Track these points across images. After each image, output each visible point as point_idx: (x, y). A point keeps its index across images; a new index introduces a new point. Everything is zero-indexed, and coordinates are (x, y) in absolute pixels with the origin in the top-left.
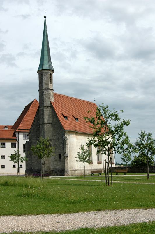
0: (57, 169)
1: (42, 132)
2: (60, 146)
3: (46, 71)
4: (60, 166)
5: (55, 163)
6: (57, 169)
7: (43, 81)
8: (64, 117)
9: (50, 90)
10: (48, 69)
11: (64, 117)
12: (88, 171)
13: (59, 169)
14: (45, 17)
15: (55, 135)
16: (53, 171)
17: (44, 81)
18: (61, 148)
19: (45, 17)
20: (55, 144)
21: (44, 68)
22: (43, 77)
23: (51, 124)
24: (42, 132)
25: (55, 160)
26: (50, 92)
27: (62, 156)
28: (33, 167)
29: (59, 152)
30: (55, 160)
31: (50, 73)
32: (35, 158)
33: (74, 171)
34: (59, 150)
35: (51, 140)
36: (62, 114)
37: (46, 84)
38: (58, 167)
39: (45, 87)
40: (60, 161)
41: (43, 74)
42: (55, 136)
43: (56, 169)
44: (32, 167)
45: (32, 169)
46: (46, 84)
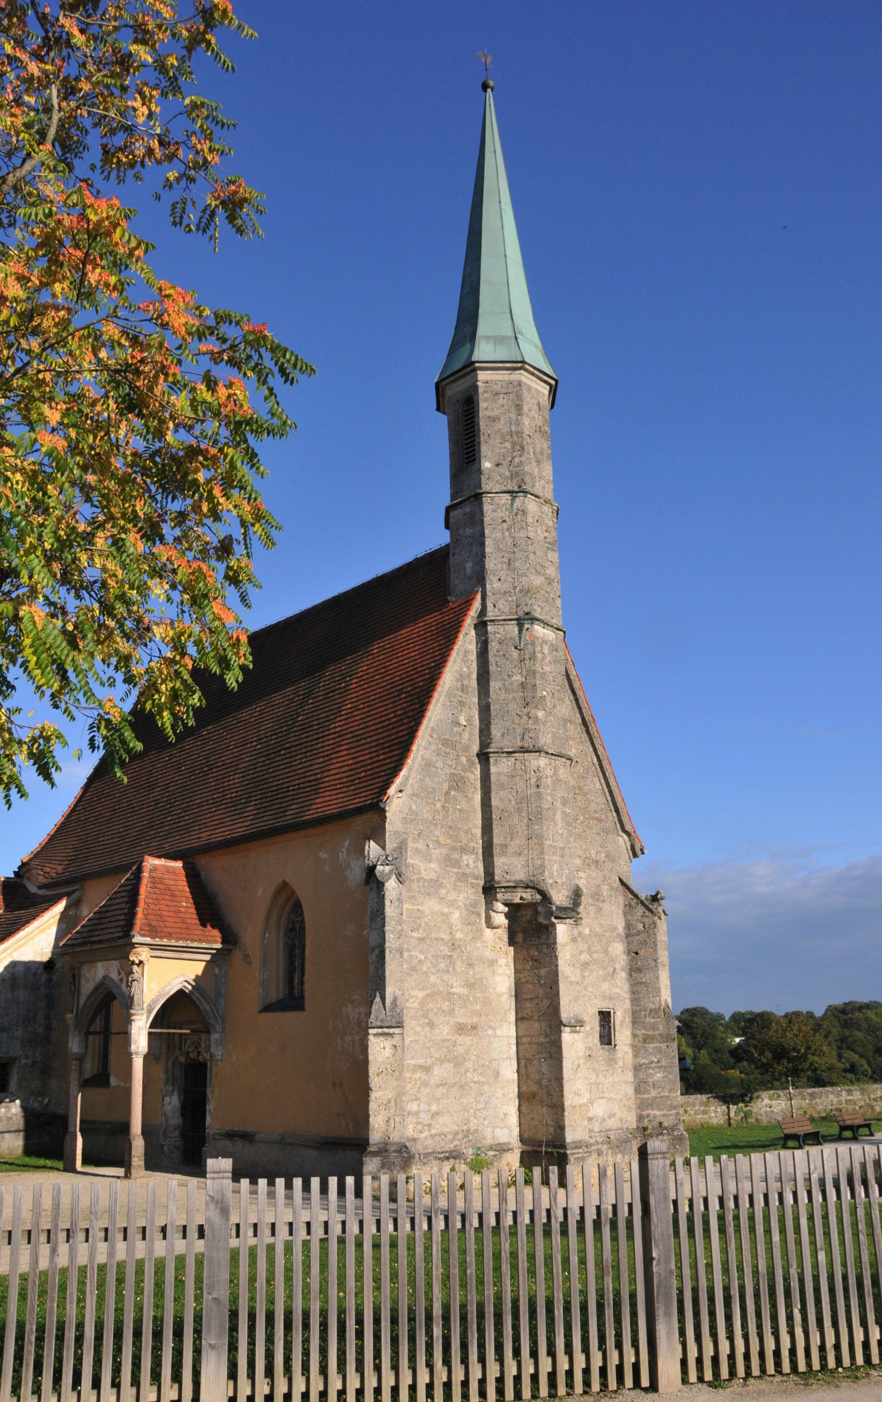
2: (606, 952)
18: (618, 966)
29: (604, 997)
32: (431, 1024)
40: (611, 1061)
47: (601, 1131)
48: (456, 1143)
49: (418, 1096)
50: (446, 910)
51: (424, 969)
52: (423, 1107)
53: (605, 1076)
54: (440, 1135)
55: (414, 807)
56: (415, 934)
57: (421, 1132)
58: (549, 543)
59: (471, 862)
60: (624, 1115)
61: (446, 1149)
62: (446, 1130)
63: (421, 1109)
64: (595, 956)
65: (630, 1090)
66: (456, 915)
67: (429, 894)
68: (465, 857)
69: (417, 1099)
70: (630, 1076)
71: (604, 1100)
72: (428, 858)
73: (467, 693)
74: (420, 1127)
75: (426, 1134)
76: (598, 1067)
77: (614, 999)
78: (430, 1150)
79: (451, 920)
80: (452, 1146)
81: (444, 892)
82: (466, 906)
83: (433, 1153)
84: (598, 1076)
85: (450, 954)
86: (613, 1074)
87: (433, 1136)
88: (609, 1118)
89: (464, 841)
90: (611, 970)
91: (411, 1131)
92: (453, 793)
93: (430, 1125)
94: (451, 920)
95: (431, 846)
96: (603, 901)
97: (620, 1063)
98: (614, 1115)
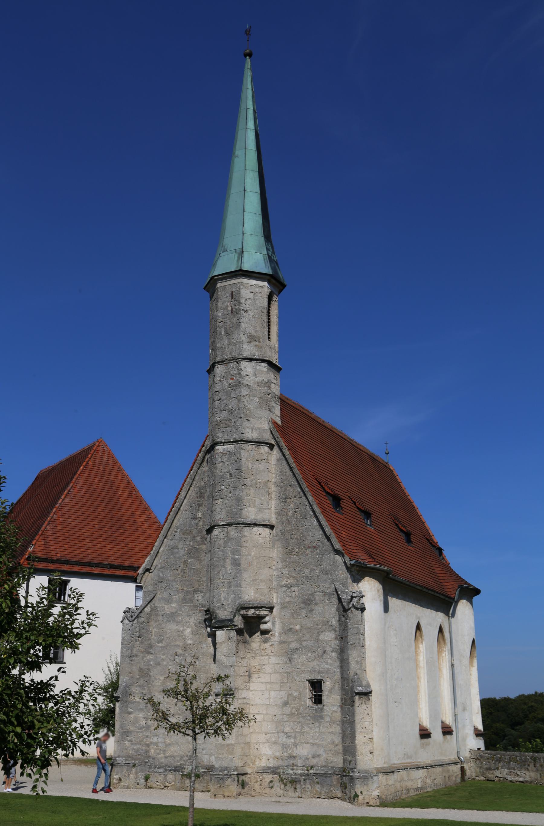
0: (299, 763)
1: (229, 562)
2: (317, 640)
4: (313, 744)
5: (287, 729)
6: (299, 763)
12: (421, 773)
13: (314, 762)
15: (292, 581)
18: (328, 649)
20: (290, 630)
23: (272, 527)
24: (229, 562)
25: (288, 710)
27: (330, 691)
28: (156, 744)
30: (288, 710)
34: (315, 663)
37: (252, 339)
38: (303, 751)
40: (318, 717)
41: (239, 292)
42: (289, 587)
43: (292, 762)
44: (148, 745)
45: (147, 752)
46: (252, 339)
47: (304, 766)
48: (182, 762)
49: (158, 734)
50: (181, 629)
51: (165, 663)
52: (160, 740)
53: (311, 728)
54: (171, 756)
55: (161, 575)
56: (160, 645)
57: (158, 754)
58: (233, 386)
59: (200, 598)
60: (330, 757)
61: (175, 765)
62: (175, 754)
63: (159, 741)
64: (305, 643)
65: (338, 739)
66: (188, 630)
67: (170, 622)
68: (196, 596)
69: (156, 736)
70: (337, 729)
71: (309, 745)
72: (169, 601)
73: (203, 498)
74: (158, 751)
75: (162, 755)
76: (303, 721)
77: (322, 673)
78: (163, 765)
79: (185, 634)
80: (179, 764)
81: (180, 618)
82: (195, 624)
83: (166, 766)
84: (303, 727)
85: (183, 653)
86: (319, 727)
87: (166, 757)
88: (314, 757)
89: (196, 587)
90: (320, 652)
91: (153, 753)
92: (190, 560)
93: (164, 751)
94: (185, 634)
95: (172, 594)
96: (316, 604)
97: (327, 719)
98: (319, 756)
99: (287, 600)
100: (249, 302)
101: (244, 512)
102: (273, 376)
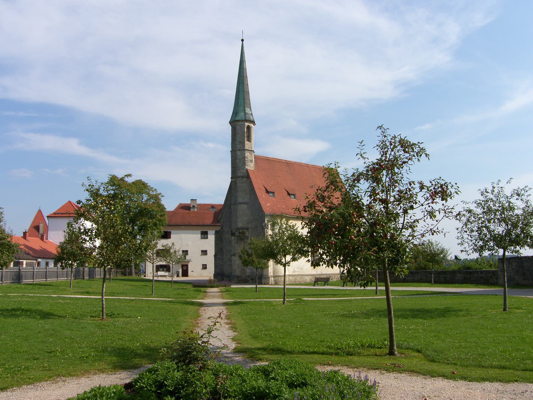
3: (241, 123)
7: (236, 139)
8: (268, 192)
9: (246, 151)
10: (244, 119)
11: (268, 192)
12: (310, 277)
14: (242, 40)
15: (253, 220)
16: (249, 276)
17: (237, 139)
19: (242, 40)
21: (237, 119)
22: (236, 131)
23: (248, 204)
26: (246, 155)
31: (246, 126)
33: (280, 278)
35: (247, 229)
36: (265, 188)
37: (240, 143)
39: (238, 146)
41: (236, 128)
42: (252, 222)
46: (240, 143)
99: (252, 226)
100: (239, 130)
101: (238, 200)
102: (249, 154)
